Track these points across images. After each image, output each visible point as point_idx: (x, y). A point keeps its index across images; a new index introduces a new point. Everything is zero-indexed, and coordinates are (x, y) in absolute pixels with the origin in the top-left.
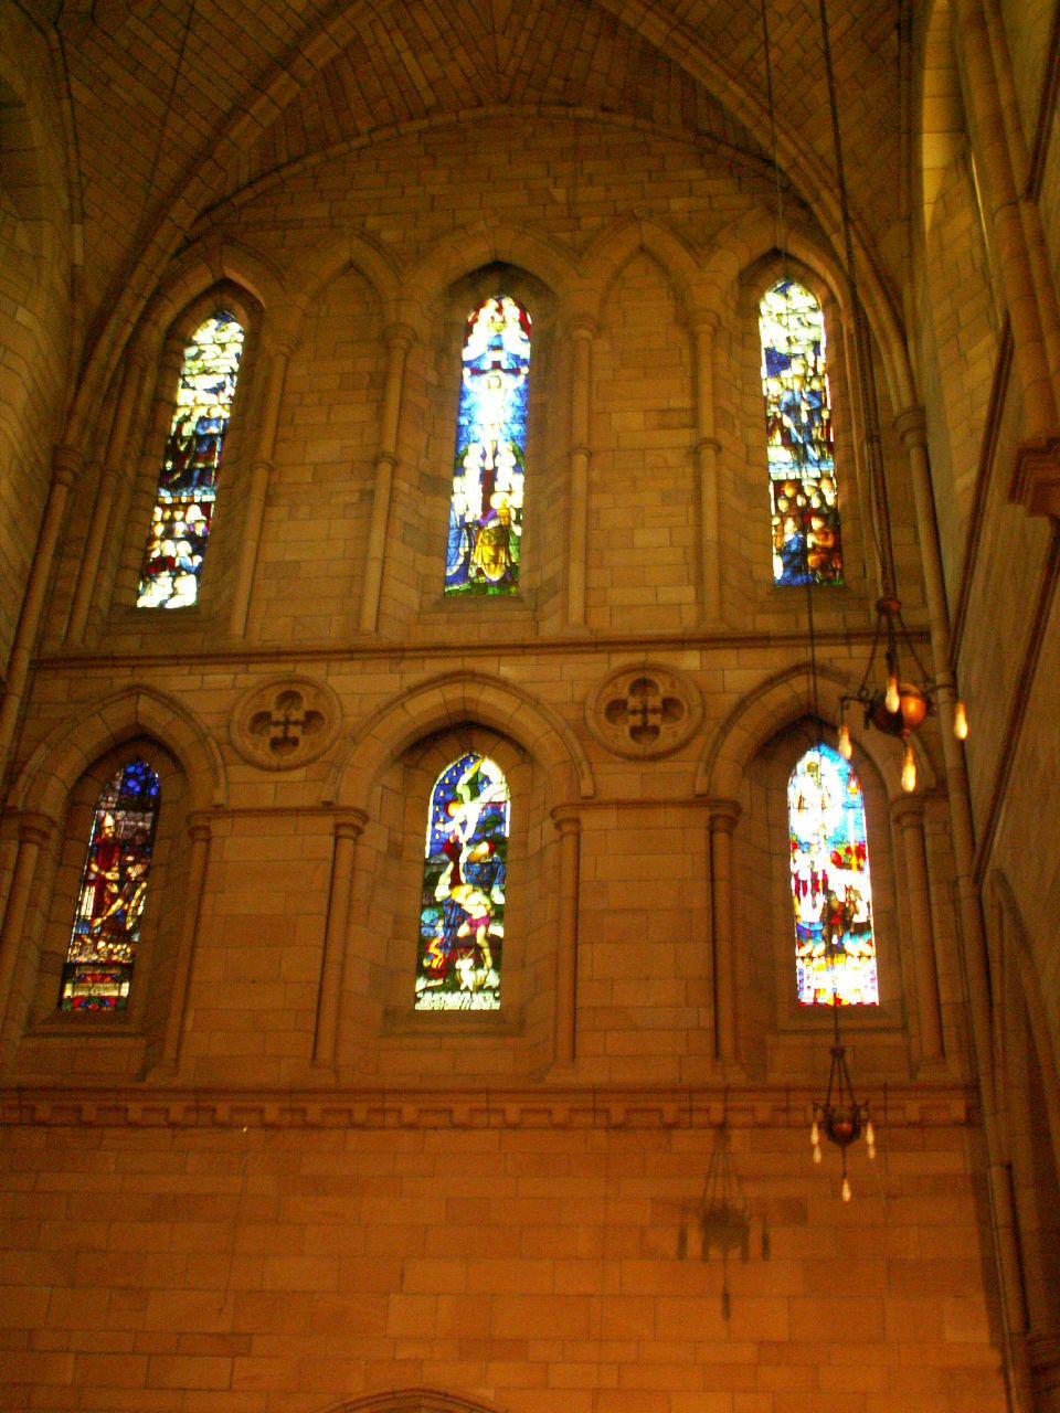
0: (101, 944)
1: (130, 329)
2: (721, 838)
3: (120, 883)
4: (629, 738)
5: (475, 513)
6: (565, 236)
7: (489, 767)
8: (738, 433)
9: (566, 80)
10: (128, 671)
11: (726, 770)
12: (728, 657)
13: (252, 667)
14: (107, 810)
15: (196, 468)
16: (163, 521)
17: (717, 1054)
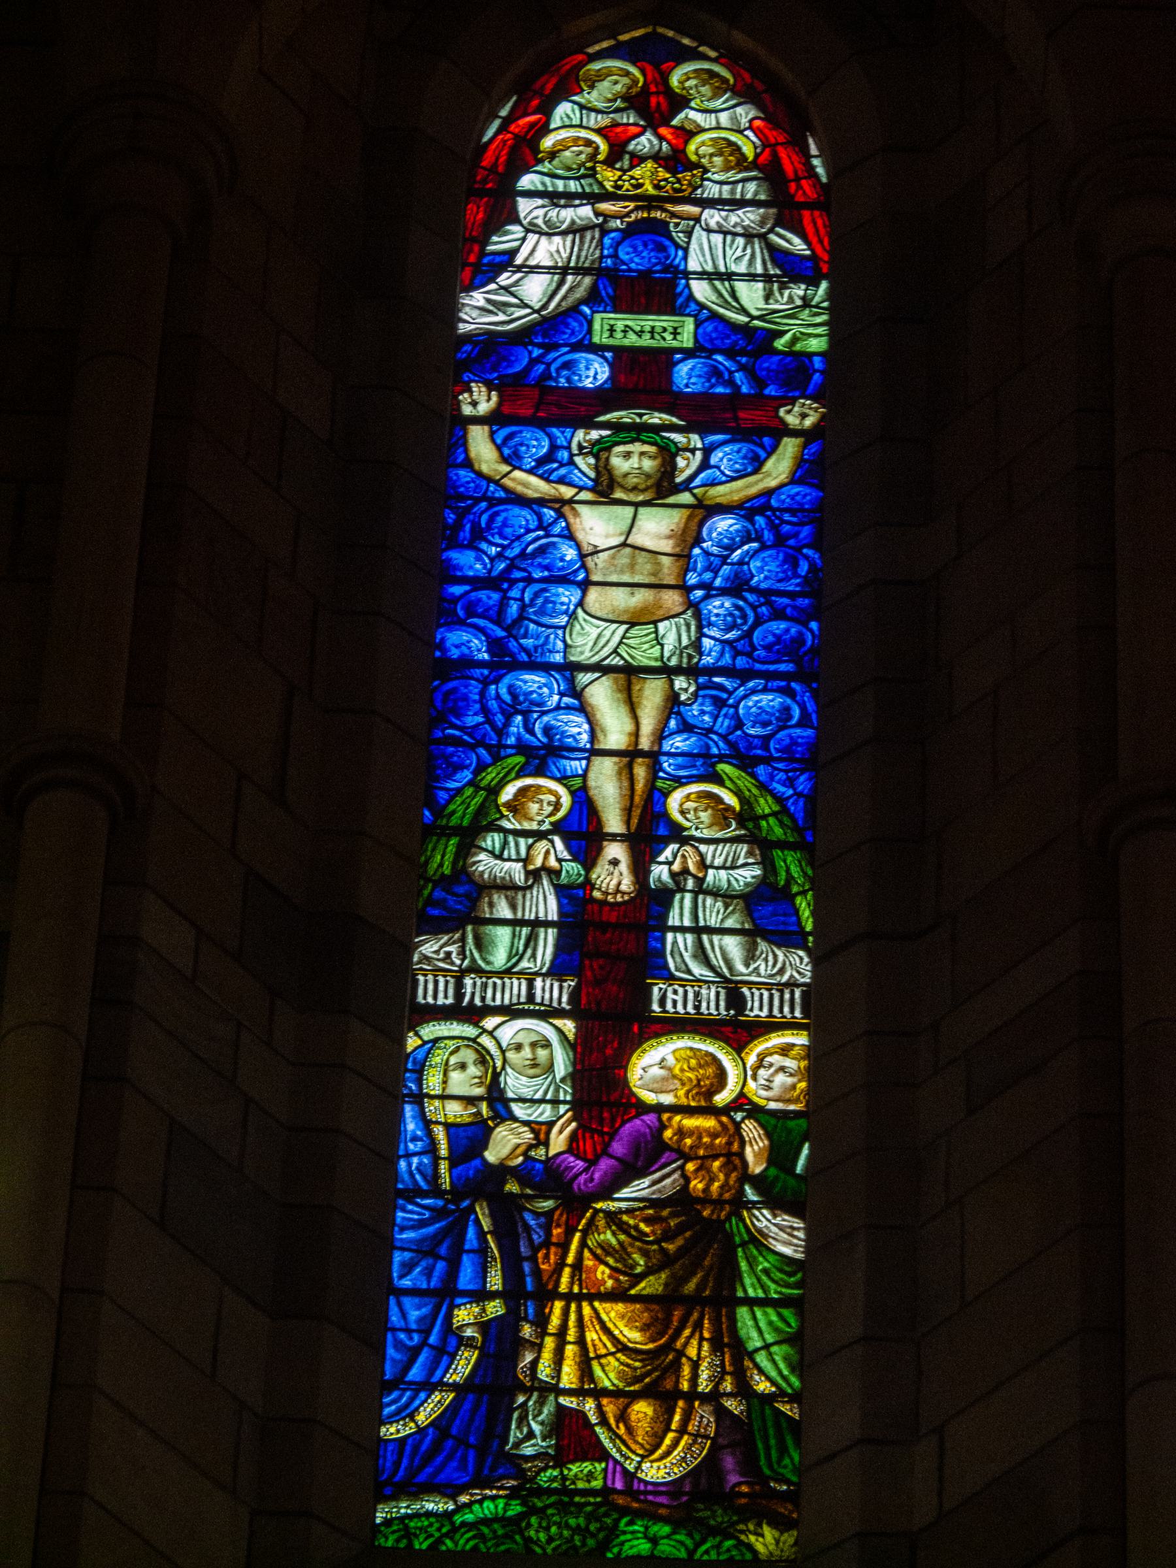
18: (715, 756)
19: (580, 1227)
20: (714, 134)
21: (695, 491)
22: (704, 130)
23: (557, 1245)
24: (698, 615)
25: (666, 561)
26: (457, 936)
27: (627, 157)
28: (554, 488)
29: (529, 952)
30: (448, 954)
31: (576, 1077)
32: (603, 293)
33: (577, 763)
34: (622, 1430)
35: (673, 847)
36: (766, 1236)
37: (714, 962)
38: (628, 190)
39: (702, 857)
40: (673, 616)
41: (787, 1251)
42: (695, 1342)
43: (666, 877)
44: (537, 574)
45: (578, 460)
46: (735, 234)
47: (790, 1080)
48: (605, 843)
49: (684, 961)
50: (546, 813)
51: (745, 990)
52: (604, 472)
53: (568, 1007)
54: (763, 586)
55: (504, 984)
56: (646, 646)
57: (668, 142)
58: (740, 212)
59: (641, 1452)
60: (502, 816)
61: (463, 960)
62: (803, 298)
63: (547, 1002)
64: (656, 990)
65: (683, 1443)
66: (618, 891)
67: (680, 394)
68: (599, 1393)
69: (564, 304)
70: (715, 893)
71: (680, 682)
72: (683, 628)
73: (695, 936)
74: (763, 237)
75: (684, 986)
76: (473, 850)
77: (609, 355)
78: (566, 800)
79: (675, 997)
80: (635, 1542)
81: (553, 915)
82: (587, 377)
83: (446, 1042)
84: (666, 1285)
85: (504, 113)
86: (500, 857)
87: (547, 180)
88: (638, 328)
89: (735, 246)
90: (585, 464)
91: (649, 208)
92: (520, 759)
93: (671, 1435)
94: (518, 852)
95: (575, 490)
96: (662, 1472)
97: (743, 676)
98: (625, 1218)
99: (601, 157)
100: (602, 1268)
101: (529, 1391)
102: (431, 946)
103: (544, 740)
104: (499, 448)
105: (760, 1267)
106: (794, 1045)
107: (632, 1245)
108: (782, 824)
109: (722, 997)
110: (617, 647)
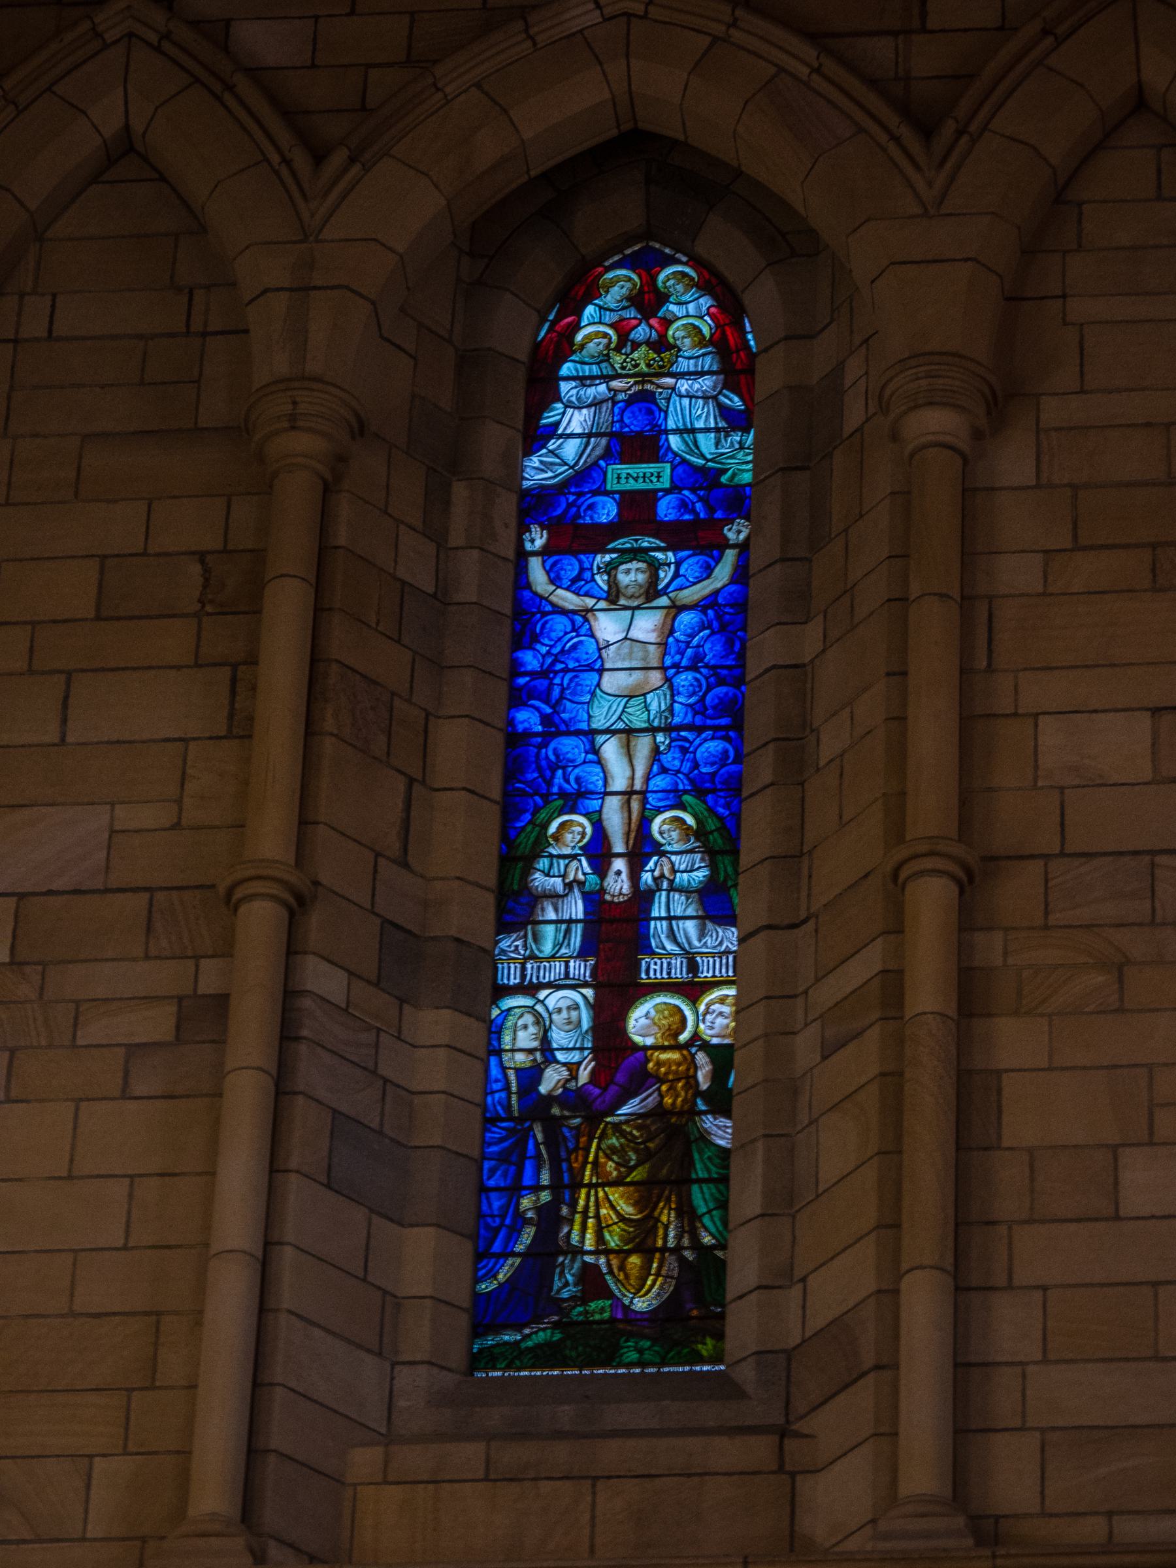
18: (681, 791)
19: (596, 1136)
20: (684, 321)
21: (671, 595)
22: (679, 318)
23: (582, 1149)
24: (671, 687)
25: (652, 648)
26: (522, 933)
27: (629, 343)
28: (582, 600)
29: (566, 942)
30: (517, 947)
31: (595, 1029)
32: (614, 450)
33: (595, 801)
34: (622, 1277)
35: (655, 858)
36: (709, 1134)
37: (680, 940)
38: (630, 370)
39: (673, 864)
40: (656, 689)
41: (722, 1143)
42: (666, 1212)
43: (650, 881)
44: (572, 665)
45: (597, 577)
46: (697, 398)
47: (726, 1021)
48: (613, 859)
49: (661, 941)
50: (577, 840)
51: (698, 959)
52: (613, 585)
53: (589, 980)
54: (713, 662)
55: (550, 966)
56: (639, 713)
57: (656, 331)
58: (700, 380)
59: (633, 1291)
60: (550, 845)
61: (526, 950)
62: (740, 443)
63: (577, 977)
64: (643, 963)
65: (658, 1283)
66: (620, 894)
67: (662, 522)
68: (608, 1252)
69: (588, 460)
70: (681, 890)
71: (660, 738)
72: (662, 697)
73: (668, 922)
74: (715, 398)
75: (660, 959)
76: (532, 871)
77: (617, 496)
78: (589, 830)
79: (655, 967)
80: (630, 1354)
81: (581, 916)
82: (603, 514)
83: (516, 1010)
84: (649, 1172)
85: (551, 317)
86: (548, 875)
87: (578, 366)
88: (635, 475)
89: (697, 408)
90: (601, 580)
91: (643, 382)
92: (560, 802)
93: (651, 1278)
94: (559, 871)
95: (594, 601)
96: (645, 1305)
97: (699, 729)
98: (624, 1127)
99: (612, 346)
100: (610, 1163)
101: (565, 1254)
102: (506, 943)
103: (575, 786)
104: (548, 573)
105: (706, 1156)
106: (728, 996)
107: (628, 1146)
108: (722, 837)
109: (684, 965)
110: (621, 715)
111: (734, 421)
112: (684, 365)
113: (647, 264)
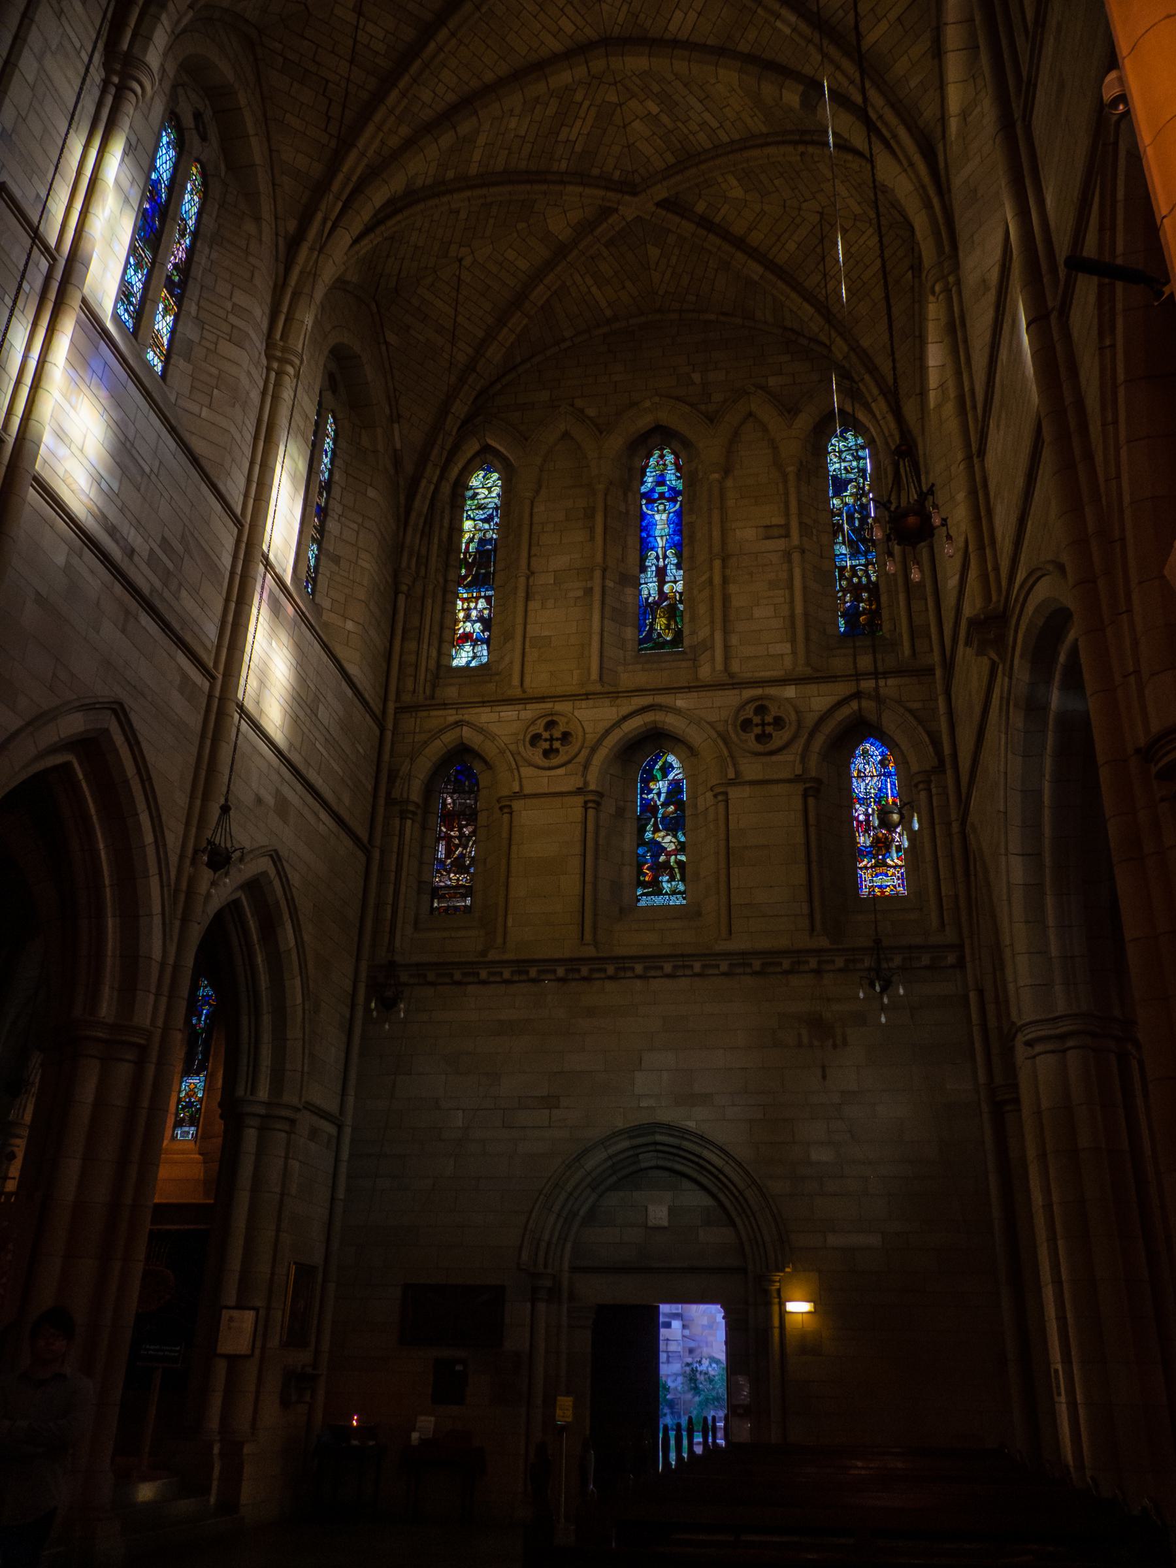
0: (452, 875)
1: (432, 487)
2: (811, 801)
3: (459, 838)
4: (755, 742)
5: (654, 596)
6: (703, 407)
7: (671, 758)
8: (815, 538)
9: (697, 296)
10: (453, 712)
11: (814, 759)
12: (812, 689)
13: (528, 706)
14: (447, 793)
15: (480, 574)
16: (463, 609)
17: (812, 929)
97: (674, 535)
111: (678, 478)
112: (669, 468)
113: (662, 450)
